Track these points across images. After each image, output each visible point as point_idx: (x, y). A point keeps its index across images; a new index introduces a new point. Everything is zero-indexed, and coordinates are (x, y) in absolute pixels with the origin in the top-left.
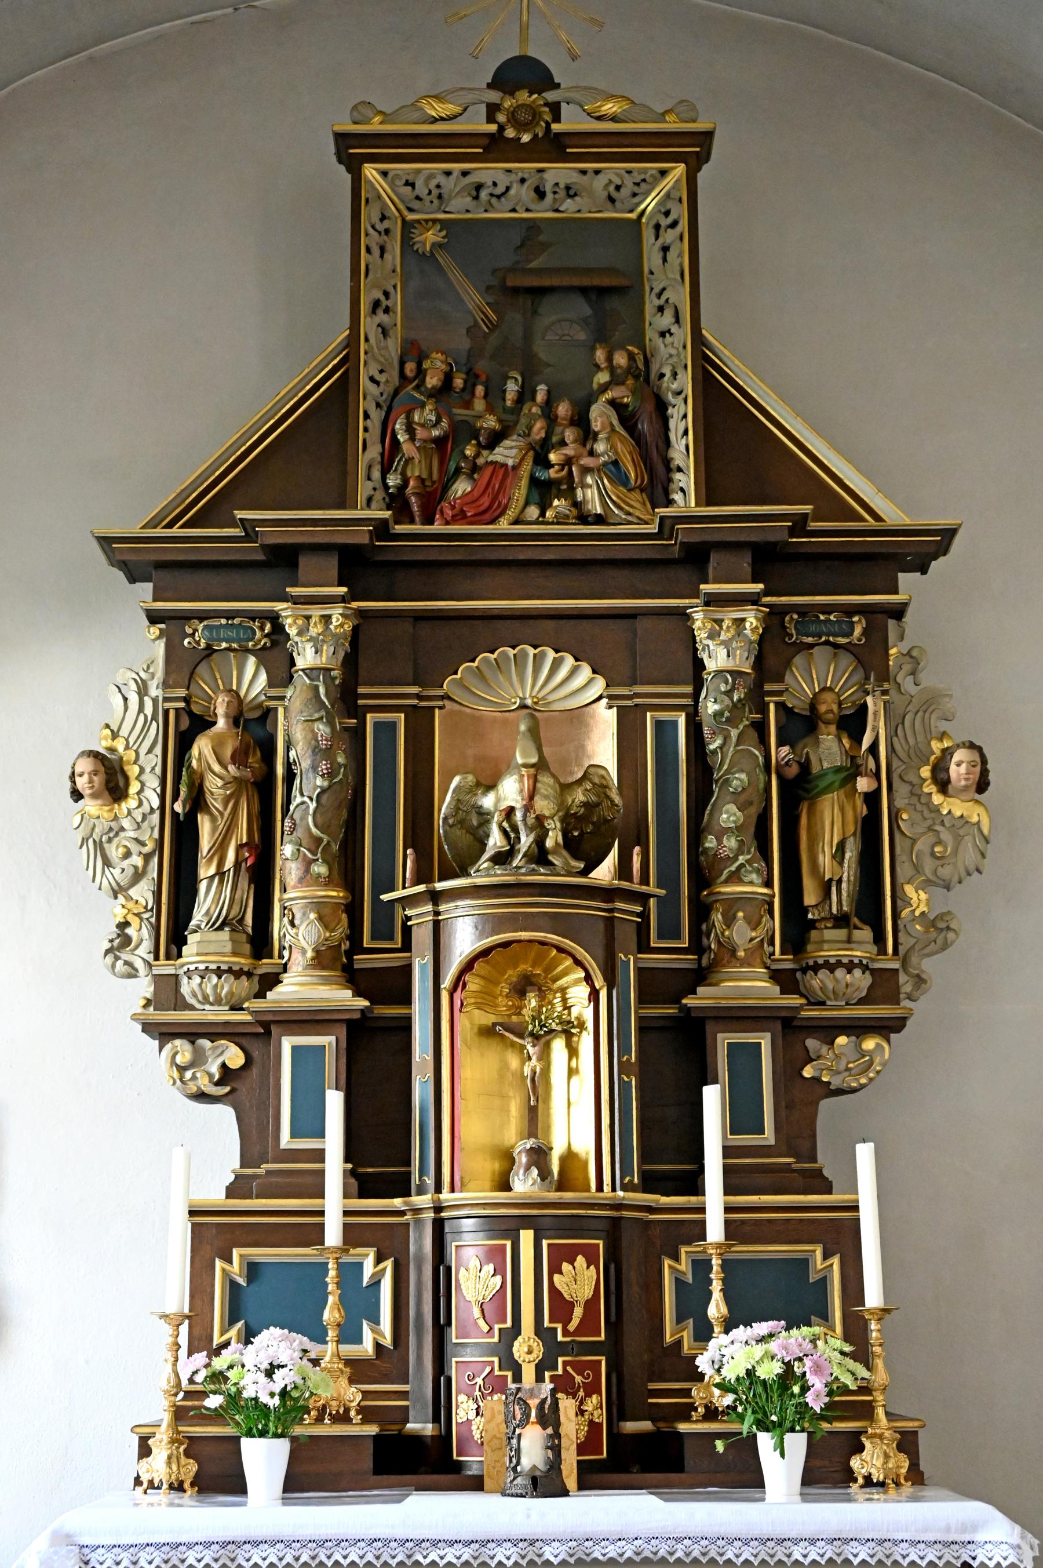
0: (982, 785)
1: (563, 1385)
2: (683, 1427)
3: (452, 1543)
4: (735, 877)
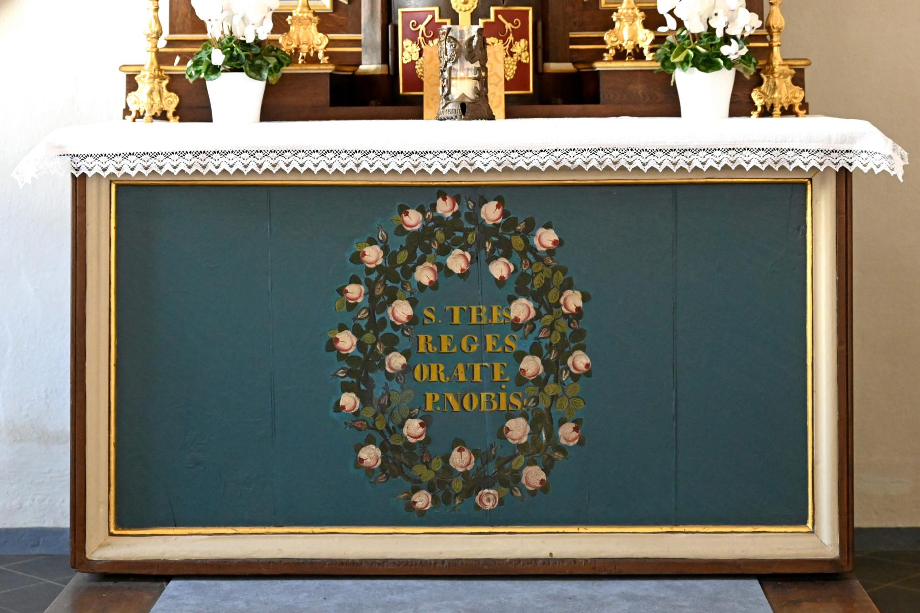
1: (496, 30)
2: (599, 66)
3: (395, 154)
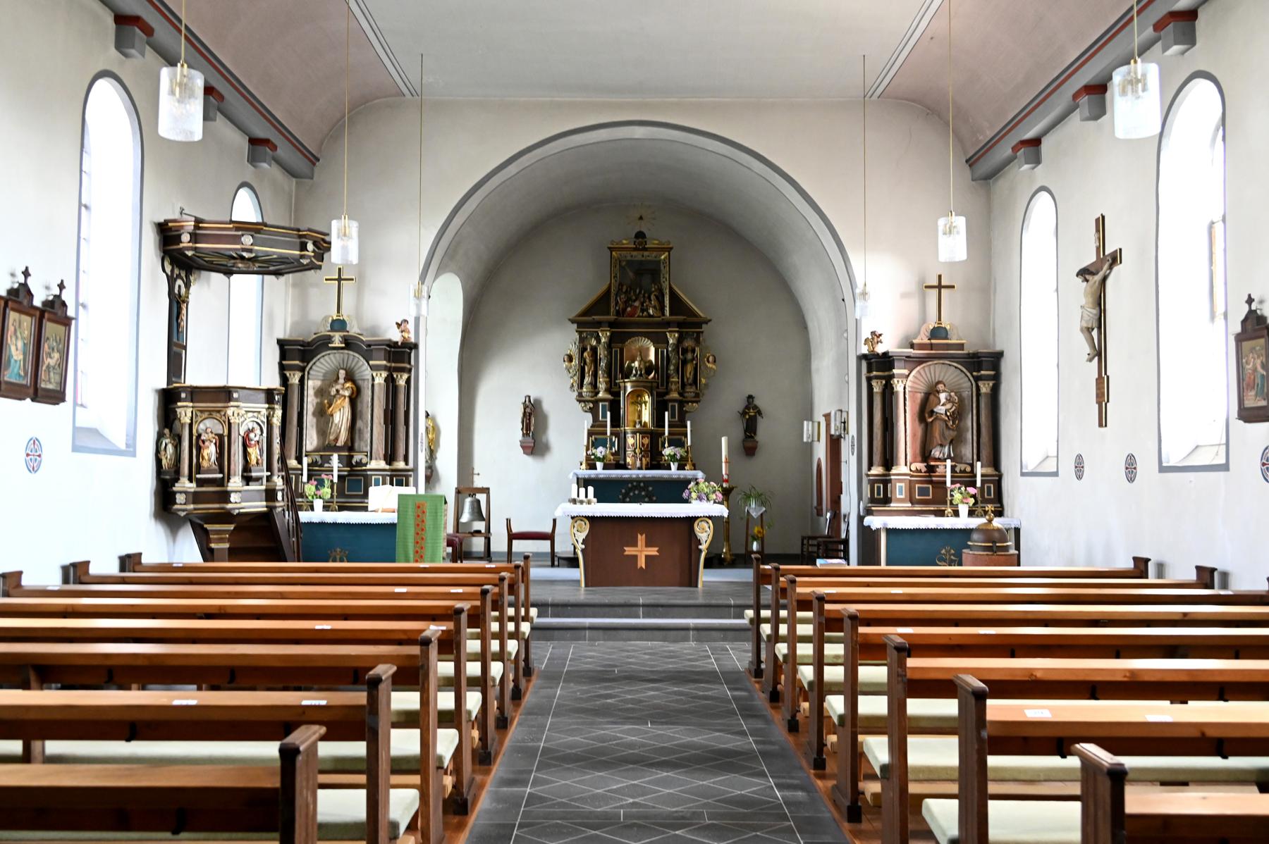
0: (715, 361)
4: (673, 378)
